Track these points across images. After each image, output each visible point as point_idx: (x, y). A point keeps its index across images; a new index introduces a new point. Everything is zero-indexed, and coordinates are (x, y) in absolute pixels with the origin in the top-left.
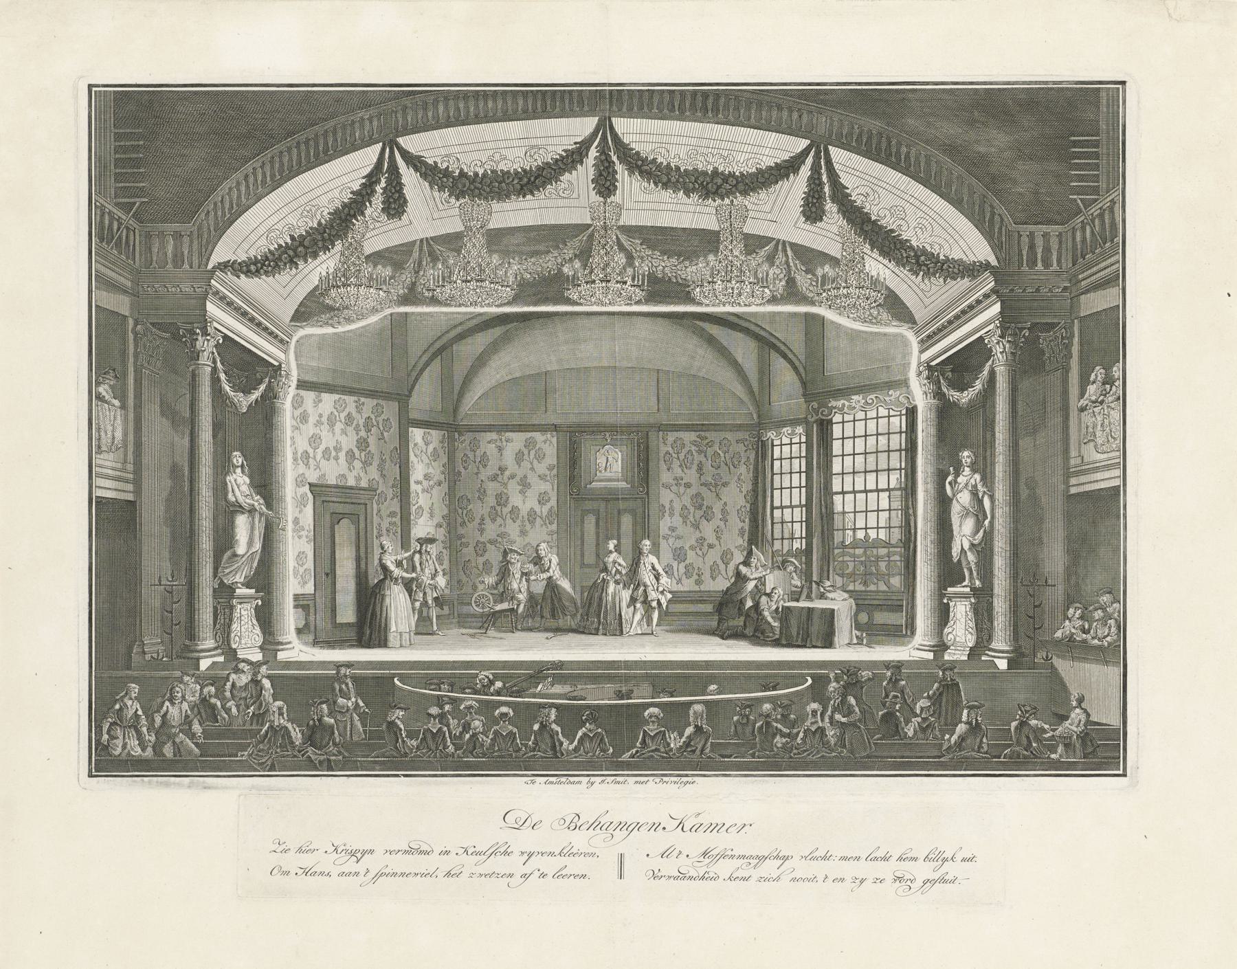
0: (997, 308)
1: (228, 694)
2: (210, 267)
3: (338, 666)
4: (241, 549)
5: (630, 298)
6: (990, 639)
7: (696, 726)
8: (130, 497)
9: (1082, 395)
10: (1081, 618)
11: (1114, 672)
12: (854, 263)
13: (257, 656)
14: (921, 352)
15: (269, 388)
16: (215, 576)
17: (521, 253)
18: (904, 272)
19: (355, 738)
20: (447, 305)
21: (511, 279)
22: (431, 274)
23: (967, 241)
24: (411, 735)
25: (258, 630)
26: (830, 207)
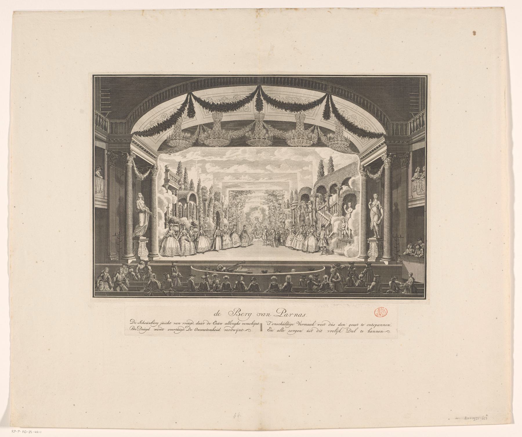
0: (386, 148)
1: (137, 271)
2: (132, 133)
3: (172, 262)
4: (142, 224)
5: (267, 144)
6: (383, 254)
7: (288, 282)
8: (106, 208)
9: (413, 176)
10: (412, 248)
11: (423, 265)
12: (340, 133)
13: (147, 259)
14: (361, 162)
15: (151, 173)
16: (133, 232)
17: (232, 129)
18: (356, 136)
19: (178, 285)
20: (208, 146)
21: (229, 138)
22: (203, 136)
23: (376, 126)
24: (196, 284)
25: (147, 250)
26: (332, 115)
